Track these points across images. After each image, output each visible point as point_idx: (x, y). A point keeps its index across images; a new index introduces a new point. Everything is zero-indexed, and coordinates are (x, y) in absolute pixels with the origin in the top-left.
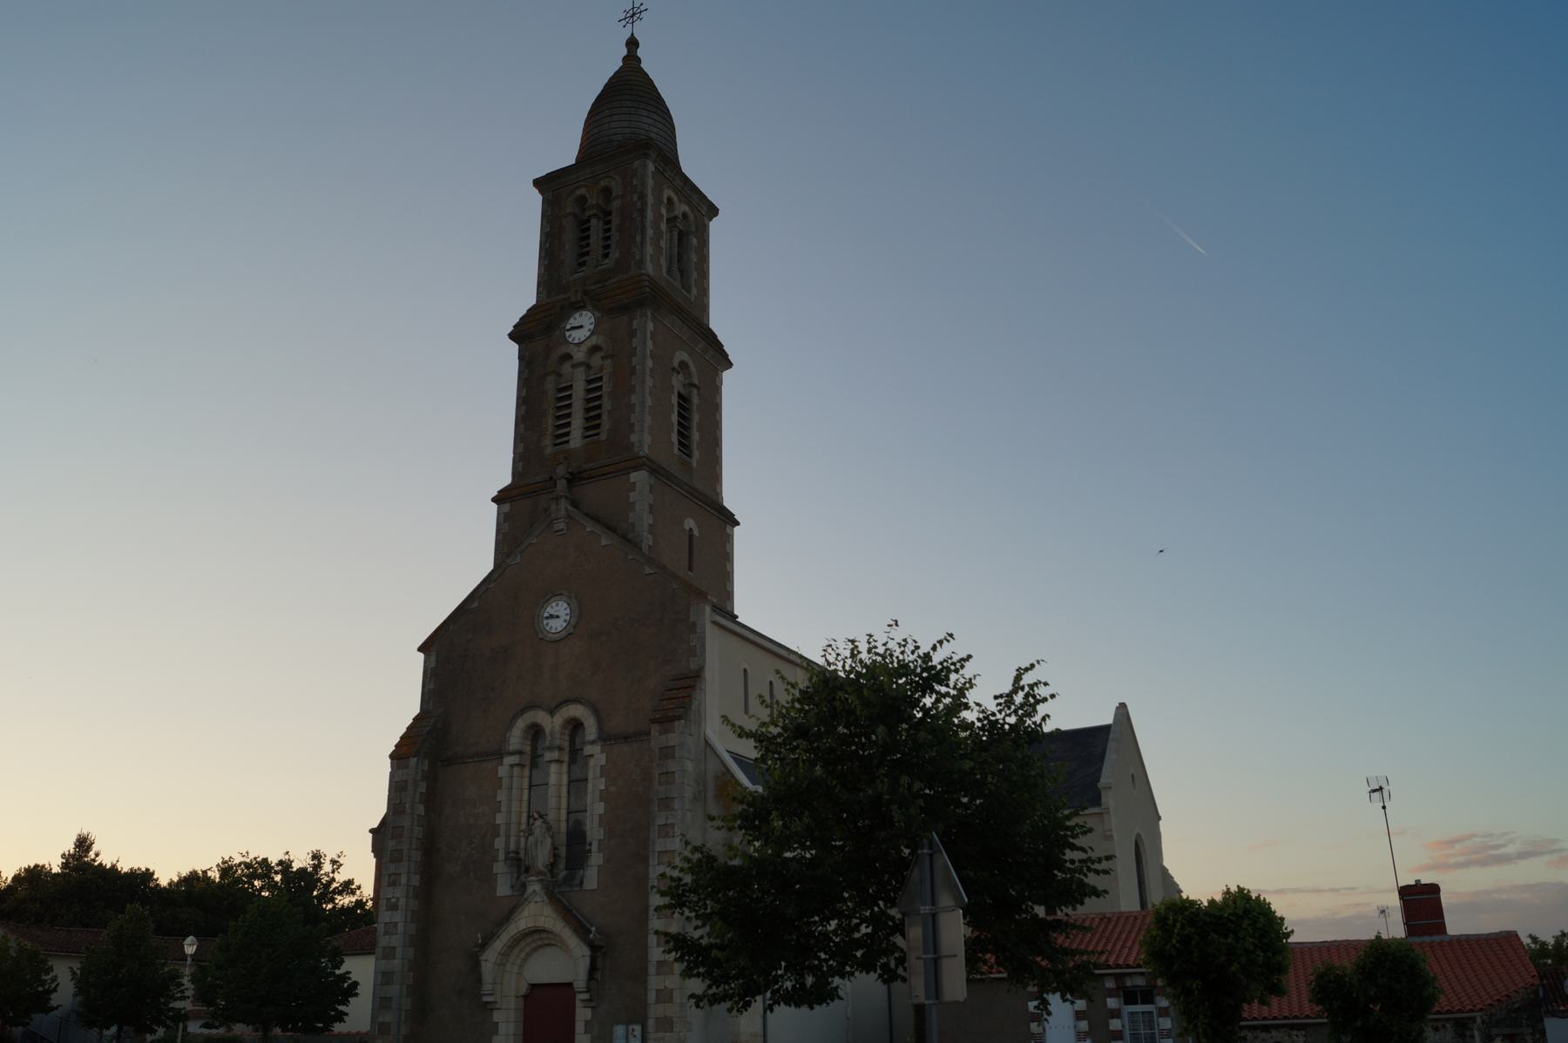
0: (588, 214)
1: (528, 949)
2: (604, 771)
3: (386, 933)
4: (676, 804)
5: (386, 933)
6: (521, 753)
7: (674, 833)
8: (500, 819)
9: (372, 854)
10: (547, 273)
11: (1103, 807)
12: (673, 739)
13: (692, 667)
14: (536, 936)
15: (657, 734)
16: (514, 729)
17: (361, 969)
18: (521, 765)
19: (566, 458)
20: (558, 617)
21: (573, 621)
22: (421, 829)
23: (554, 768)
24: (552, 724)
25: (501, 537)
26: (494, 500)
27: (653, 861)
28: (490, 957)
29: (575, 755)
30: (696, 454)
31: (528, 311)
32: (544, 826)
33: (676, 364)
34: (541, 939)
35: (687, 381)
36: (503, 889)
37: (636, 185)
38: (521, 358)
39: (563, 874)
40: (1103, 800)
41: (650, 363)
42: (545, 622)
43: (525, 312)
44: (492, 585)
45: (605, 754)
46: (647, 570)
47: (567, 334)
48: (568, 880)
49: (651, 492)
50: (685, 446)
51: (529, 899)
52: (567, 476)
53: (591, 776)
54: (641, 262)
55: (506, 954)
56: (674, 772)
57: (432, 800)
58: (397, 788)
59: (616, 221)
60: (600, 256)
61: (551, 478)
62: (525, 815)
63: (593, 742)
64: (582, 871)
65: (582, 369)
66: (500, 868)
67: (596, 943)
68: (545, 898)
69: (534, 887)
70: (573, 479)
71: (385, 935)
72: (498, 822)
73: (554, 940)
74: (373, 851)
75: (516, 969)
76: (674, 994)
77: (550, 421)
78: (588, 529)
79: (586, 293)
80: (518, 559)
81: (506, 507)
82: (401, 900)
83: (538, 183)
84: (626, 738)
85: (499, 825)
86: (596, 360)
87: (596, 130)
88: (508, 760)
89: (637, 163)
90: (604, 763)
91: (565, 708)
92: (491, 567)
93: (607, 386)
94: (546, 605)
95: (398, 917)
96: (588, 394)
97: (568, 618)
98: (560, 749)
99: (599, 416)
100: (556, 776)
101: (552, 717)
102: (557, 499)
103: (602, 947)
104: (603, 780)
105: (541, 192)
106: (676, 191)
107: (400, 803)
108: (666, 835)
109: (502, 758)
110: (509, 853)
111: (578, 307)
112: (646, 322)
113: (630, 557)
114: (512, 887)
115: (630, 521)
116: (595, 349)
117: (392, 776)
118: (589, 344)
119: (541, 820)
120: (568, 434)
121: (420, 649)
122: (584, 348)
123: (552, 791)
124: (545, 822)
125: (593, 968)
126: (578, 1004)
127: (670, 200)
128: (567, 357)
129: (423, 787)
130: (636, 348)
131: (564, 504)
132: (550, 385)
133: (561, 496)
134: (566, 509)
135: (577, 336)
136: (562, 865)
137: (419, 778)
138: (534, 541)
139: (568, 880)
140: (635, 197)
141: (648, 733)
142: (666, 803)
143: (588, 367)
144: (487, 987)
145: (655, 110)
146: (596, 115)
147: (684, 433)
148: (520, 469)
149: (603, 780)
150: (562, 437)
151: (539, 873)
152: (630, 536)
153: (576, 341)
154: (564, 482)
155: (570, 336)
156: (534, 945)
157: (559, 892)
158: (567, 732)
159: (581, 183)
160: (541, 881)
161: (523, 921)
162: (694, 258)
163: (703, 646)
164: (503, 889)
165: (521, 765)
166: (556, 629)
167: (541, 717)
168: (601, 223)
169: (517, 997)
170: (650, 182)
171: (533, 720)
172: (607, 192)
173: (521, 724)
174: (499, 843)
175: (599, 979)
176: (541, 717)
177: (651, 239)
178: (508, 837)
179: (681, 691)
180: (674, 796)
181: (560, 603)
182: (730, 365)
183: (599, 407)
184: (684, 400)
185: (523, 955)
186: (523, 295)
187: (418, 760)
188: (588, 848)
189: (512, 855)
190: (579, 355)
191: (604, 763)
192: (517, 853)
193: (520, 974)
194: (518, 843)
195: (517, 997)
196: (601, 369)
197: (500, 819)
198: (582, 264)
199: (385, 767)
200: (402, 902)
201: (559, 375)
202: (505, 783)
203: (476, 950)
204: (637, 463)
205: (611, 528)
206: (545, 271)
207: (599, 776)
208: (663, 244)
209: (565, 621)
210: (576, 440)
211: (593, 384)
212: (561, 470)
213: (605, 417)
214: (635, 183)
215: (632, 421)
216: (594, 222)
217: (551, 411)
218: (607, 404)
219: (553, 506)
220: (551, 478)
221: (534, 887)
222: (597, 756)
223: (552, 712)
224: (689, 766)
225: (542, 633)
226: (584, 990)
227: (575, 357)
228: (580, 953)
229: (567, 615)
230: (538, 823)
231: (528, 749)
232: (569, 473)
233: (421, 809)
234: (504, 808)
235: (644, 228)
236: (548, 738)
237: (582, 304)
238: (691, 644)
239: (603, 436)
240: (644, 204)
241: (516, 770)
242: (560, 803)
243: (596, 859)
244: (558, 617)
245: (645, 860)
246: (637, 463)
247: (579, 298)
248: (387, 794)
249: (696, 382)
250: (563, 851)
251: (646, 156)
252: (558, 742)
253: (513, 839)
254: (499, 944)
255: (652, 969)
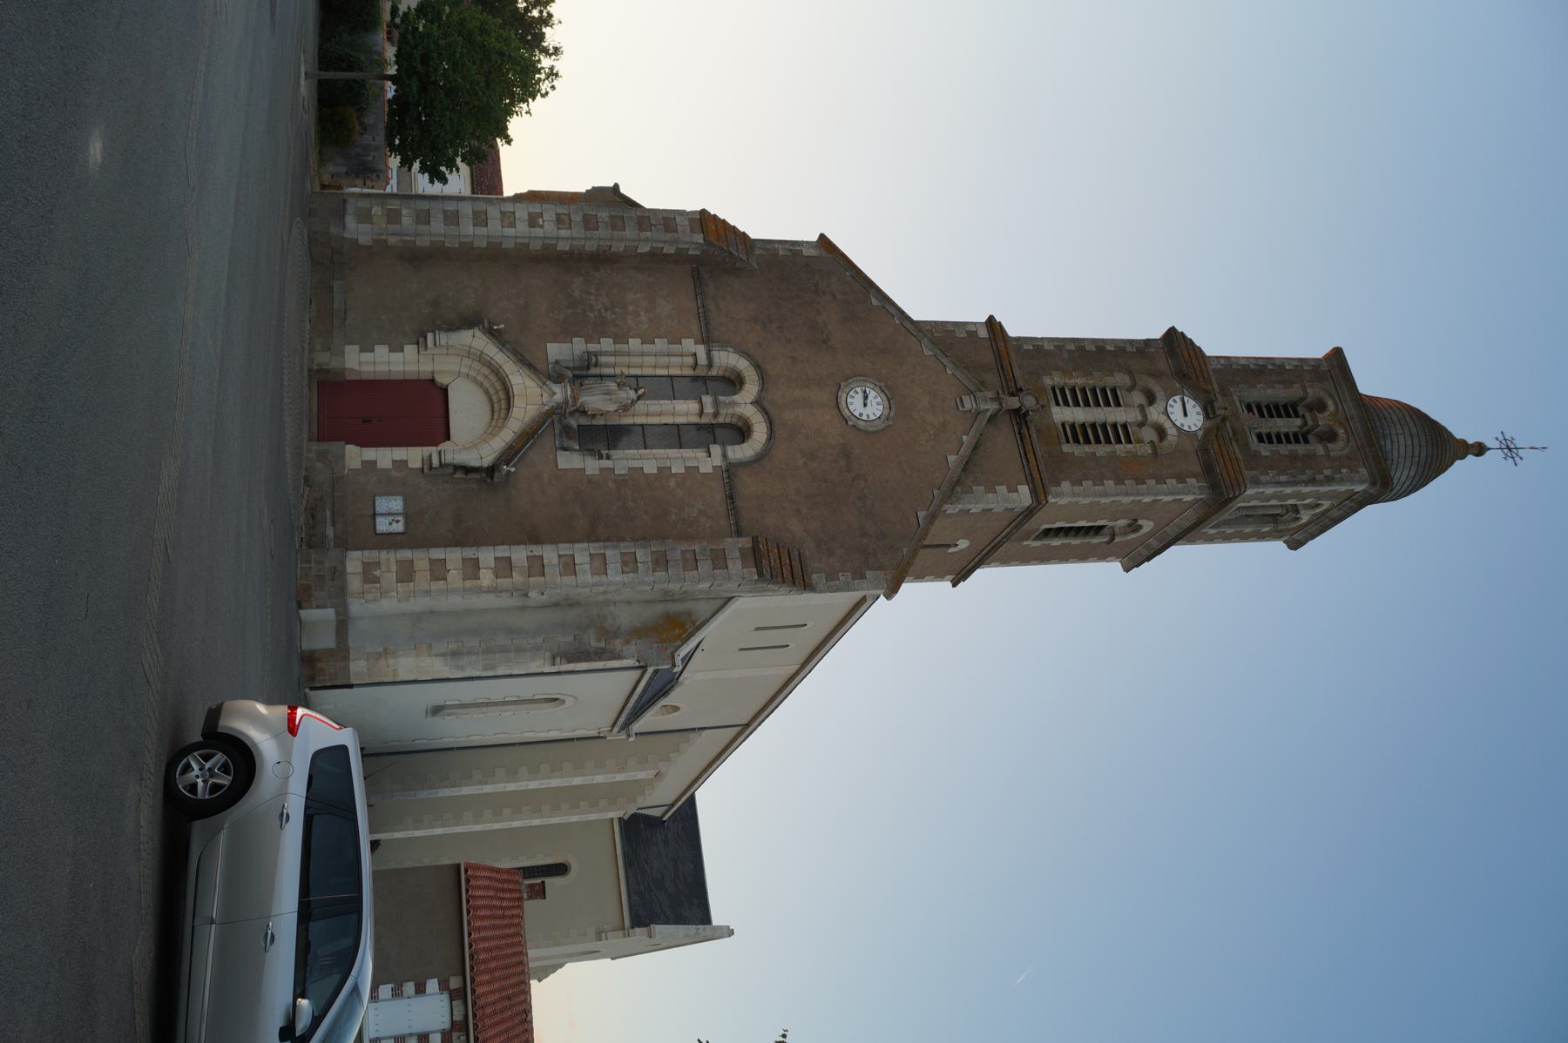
0: (1307, 415)
1: (487, 384)
2: (692, 471)
3: (503, 214)
4: (660, 574)
5: (503, 214)
6: (710, 365)
7: (628, 573)
8: (634, 343)
9: (590, 188)
10: (1240, 367)
11: (631, 931)
12: (735, 566)
13: (814, 576)
14: (502, 395)
15: (740, 546)
16: (737, 356)
17: (459, 182)
18: (695, 366)
19: (1043, 406)
20: (865, 405)
21: (861, 424)
22: (622, 249)
23: (693, 406)
24: (744, 404)
25: (951, 328)
26: (991, 318)
27: (594, 548)
28: (475, 339)
29: (706, 433)
30: (1038, 544)
31: (1199, 348)
32: (630, 401)
33: (1140, 522)
34: (500, 410)
35: (1117, 530)
36: (556, 351)
37: (1341, 473)
38: (1148, 342)
39: (573, 423)
40: (637, 930)
41: (1147, 499)
42: (858, 389)
43: (1198, 345)
44: (897, 321)
45: (711, 471)
46: (921, 514)
47: (1177, 398)
48: (567, 431)
49: (1006, 509)
50: (1047, 533)
51: (545, 387)
52: (1024, 410)
53: (687, 453)
54: (1257, 483)
55: (481, 358)
56: (697, 569)
57: (655, 259)
58: (668, 220)
59: (1300, 449)
60: (1258, 431)
61: (1021, 390)
62: (638, 372)
63: (724, 456)
64: (577, 447)
65: (1140, 418)
66: (579, 346)
67: (496, 474)
68: (546, 408)
69: (560, 393)
70: (1019, 416)
71: (501, 212)
72: (630, 340)
73: (499, 417)
74: (593, 188)
75: (464, 370)
76: (442, 582)
77: (1079, 381)
78: (964, 438)
79: (1224, 419)
80: (928, 353)
81: (983, 333)
82: (541, 230)
83: (1337, 355)
84: (731, 497)
85: (628, 343)
86: (1148, 434)
87: (1395, 418)
88: (701, 351)
89: (1364, 471)
90: (702, 470)
91: (763, 420)
92: (916, 315)
93: (1121, 449)
94: (878, 389)
95: (522, 228)
96: (1080, 390)
97: (864, 417)
98: (716, 415)
99: (1087, 441)
100: (684, 411)
101: (751, 403)
102: (997, 399)
103: (492, 478)
104: (683, 471)
105: (1328, 357)
106: (1327, 511)
107: (651, 224)
108: (624, 563)
109: (703, 343)
110: (596, 356)
111: (1208, 410)
112: (1194, 494)
113: (936, 492)
114: (557, 362)
115: (974, 488)
116: (1161, 432)
117: (682, 213)
118: (1167, 425)
119: (635, 398)
120: (1066, 404)
121: (822, 236)
122: (1162, 419)
123: (667, 405)
124: (633, 402)
125: (467, 470)
126: (427, 450)
127: (1318, 505)
128: (1151, 399)
129: (669, 250)
130: (1165, 483)
131: (992, 407)
132: (1120, 379)
133: (1001, 404)
134: (988, 410)
135: (1175, 409)
136: (584, 421)
137: (679, 246)
138: (949, 372)
139: (567, 431)
140: (1328, 472)
141: (739, 534)
142: (661, 562)
143: (1141, 425)
144: (443, 338)
145: (1414, 483)
146: (1411, 417)
147: (1058, 532)
148: (1025, 347)
149: (683, 471)
150: (1065, 396)
151: (575, 399)
152: (958, 489)
153: (1169, 409)
154: (1017, 405)
155: (1175, 401)
156: (492, 391)
157: (553, 421)
158: (734, 421)
159: (1340, 406)
160: (566, 402)
161: (521, 381)
162: (1248, 530)
163: (838, 590)
164: (556, 351)
165: (695, 366)
166: (852, 404)
167: (751, 390)
168: (1296, 429)
169: (432, 373)
170: (1342, 488)
171: (747, 381)
172: (1330, 437)
173: (742, 364)
174: (607, 344)
175: (455, 476)
176: (751, 390)
177: (1281, 492)
178: (614, 354)
179: (789, 568)
180: (670, 571)
181: (881, 407)
182: (1127, 570)
183: (1098, 441)
184: (1098, 530)
185: (480, 378)
186: (1215, 342)
187: (701, 244)
188: (604, 452)
189: (594, 358)
190: (1154, 414)
191: (702, 470)
192: (596, 365)
193: (459, 374)
194: (607, 365)
195: (432, 373)
196: (1140, 441)
197: (634, 343)
198: (1249, 408)
199: (689, 203)
200: (538, 232)
201: (1131, 389)
202: (675, 348)
203: (486, 325)
204: (1039, 495)
205: (967, 466)
206: (1242, 365)
207: (687, 465)
208: (1273, 502)
209: (861, 414)
210: (1063, 414)
211: (1121, 433)
212: (1029, 402)
213: (1087, 448)
214: (1343, 471)
215: (1084, 483)
216: (1298, 422)
217: (1091, 382)
218: (1102, 450)
219: (990, 394)
220: (1021, 390)
221: (560, 393)
222: (708, 461)
223: (757, 403)
224: (705, 585)
225: (846, 386)
226: (443, 461)
227: (1151, 408)
228: (484, 455)
229: (868, 416)
230: (632, 395)
231: (714, 372)
232: (1028, 411)
233: (644, 249)
234: (647, 348)
235: (1294, 484)
236: (727, 399)
237: (1211, 416)
238: (840, 574)
239: (1066, 448)
240: (1321, 483)
241: (690, 360)
242: (654, 415)
243: (592, 466)
244: (865, 405)
245: (591, 537)
246: (1039, 495)
247: (1218, 413)
248: (661, 208)
249: (1117, 539)
250: (600, 421)
251: (1374, 483)
252: (723, 411)
253: (611, 359)
254: (492, 350)
255: (469, 552)
